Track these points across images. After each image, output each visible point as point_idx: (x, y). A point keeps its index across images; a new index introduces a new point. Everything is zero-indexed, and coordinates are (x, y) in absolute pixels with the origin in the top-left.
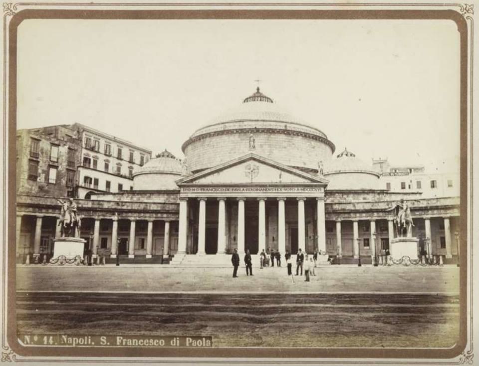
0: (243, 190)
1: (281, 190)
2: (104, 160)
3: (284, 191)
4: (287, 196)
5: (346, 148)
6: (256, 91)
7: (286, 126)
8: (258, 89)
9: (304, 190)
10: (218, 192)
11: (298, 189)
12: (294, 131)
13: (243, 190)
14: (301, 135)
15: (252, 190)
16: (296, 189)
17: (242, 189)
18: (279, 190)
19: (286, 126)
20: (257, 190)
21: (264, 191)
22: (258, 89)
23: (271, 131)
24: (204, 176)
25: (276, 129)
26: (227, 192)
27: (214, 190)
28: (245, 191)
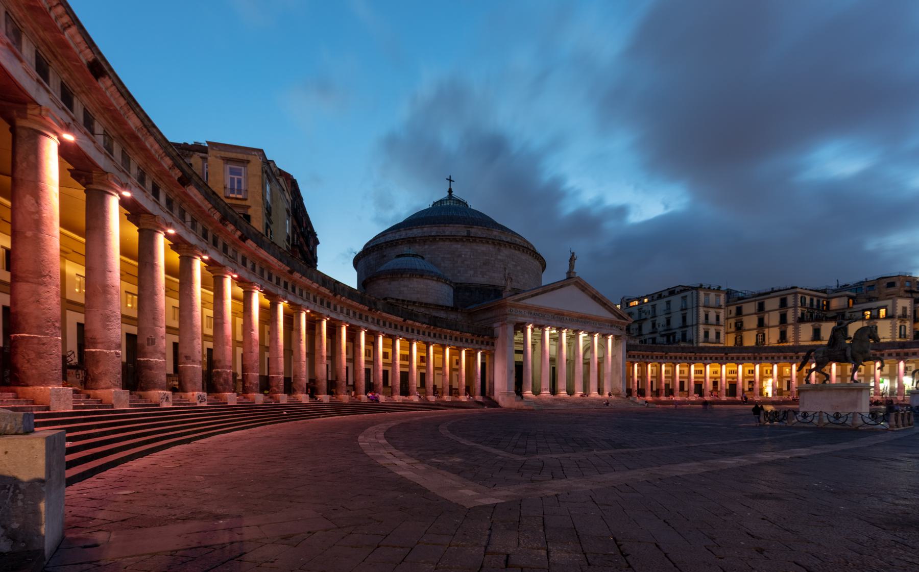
6: (448, 194)
8: (450, 191)
13: (566, 319)
22: (450, 191)
24: (533, 296)
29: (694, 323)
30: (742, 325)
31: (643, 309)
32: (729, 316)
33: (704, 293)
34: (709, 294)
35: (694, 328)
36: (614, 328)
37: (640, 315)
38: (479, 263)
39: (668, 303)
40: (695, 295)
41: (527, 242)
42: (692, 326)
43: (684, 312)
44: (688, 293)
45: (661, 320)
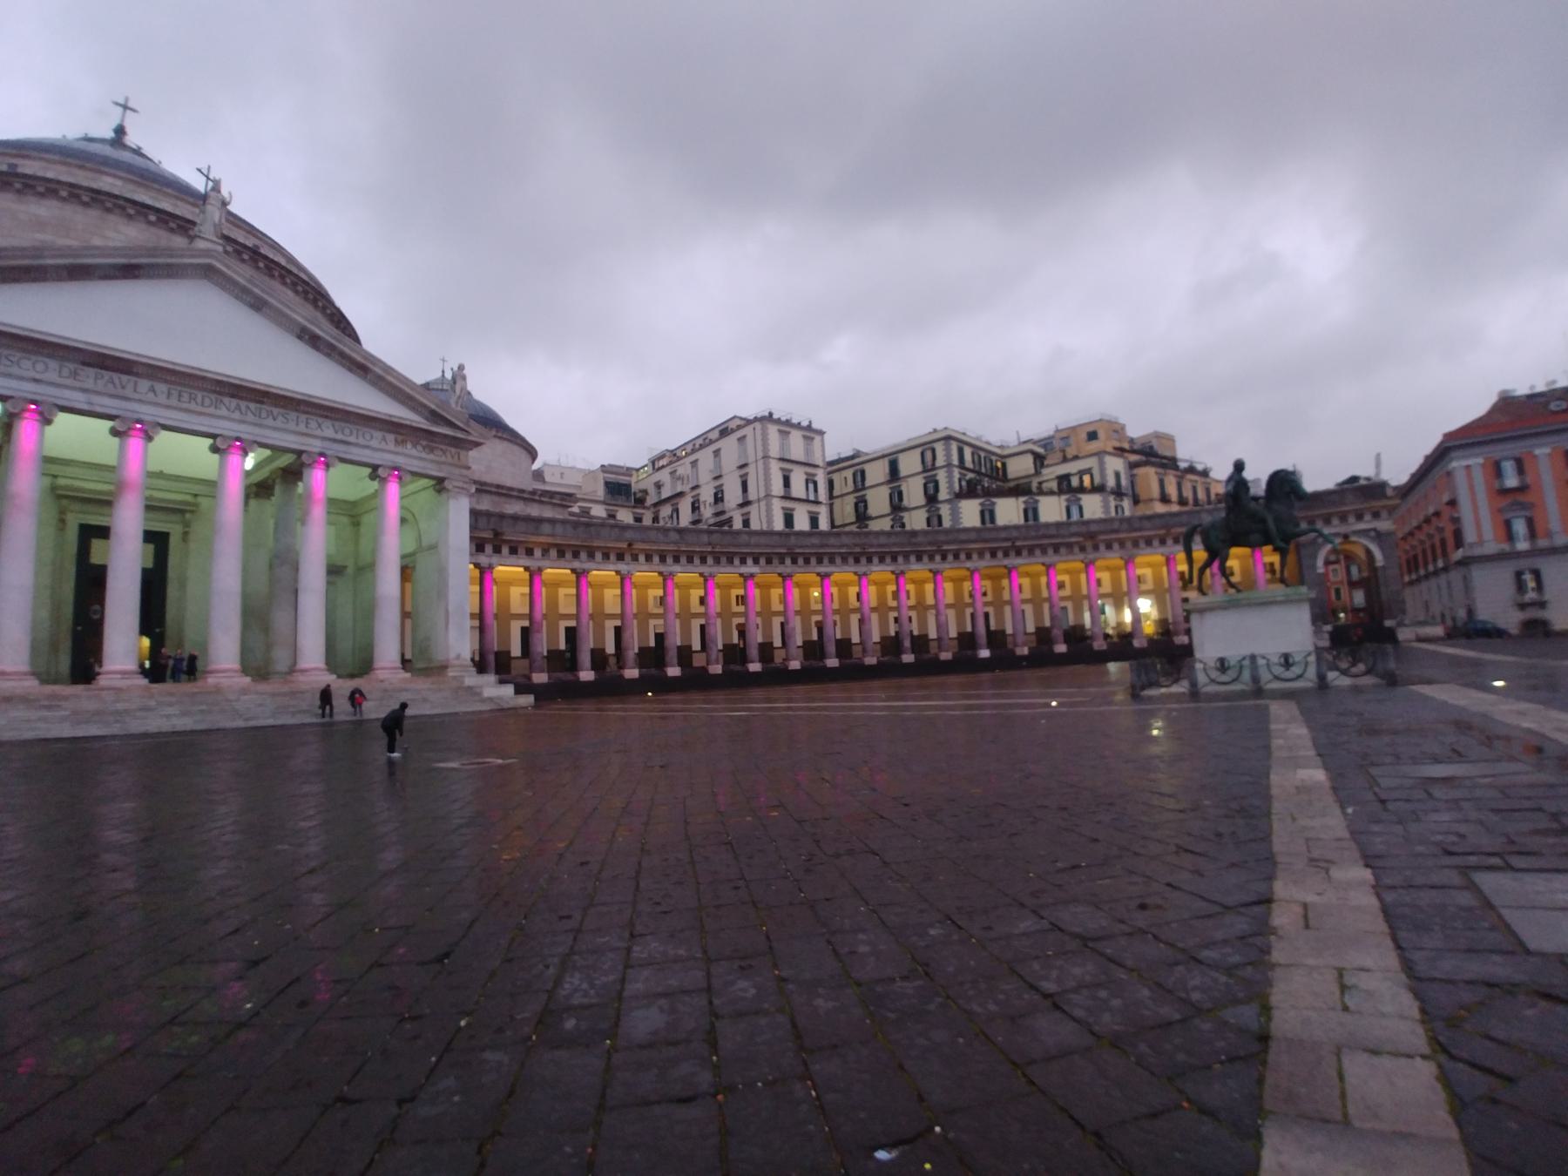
1: (320, 426)
5: (443, 372)
16: (378, 434)
17: (144, 385)
26: (69, 382)
29: (762, 494)
30: (866, 507)
31: (678, 473)
32: (845, 491)
33: (780, 431)
34: (789, 433)
35: (763, 503)
36: (414, 452)
37: (674, 486)
39: (717, 453)
40: (759, 432)
41: (251, 230)
42: (759, 500)
43: (743, 471)
44: (748, 431)
45: (707, 495)
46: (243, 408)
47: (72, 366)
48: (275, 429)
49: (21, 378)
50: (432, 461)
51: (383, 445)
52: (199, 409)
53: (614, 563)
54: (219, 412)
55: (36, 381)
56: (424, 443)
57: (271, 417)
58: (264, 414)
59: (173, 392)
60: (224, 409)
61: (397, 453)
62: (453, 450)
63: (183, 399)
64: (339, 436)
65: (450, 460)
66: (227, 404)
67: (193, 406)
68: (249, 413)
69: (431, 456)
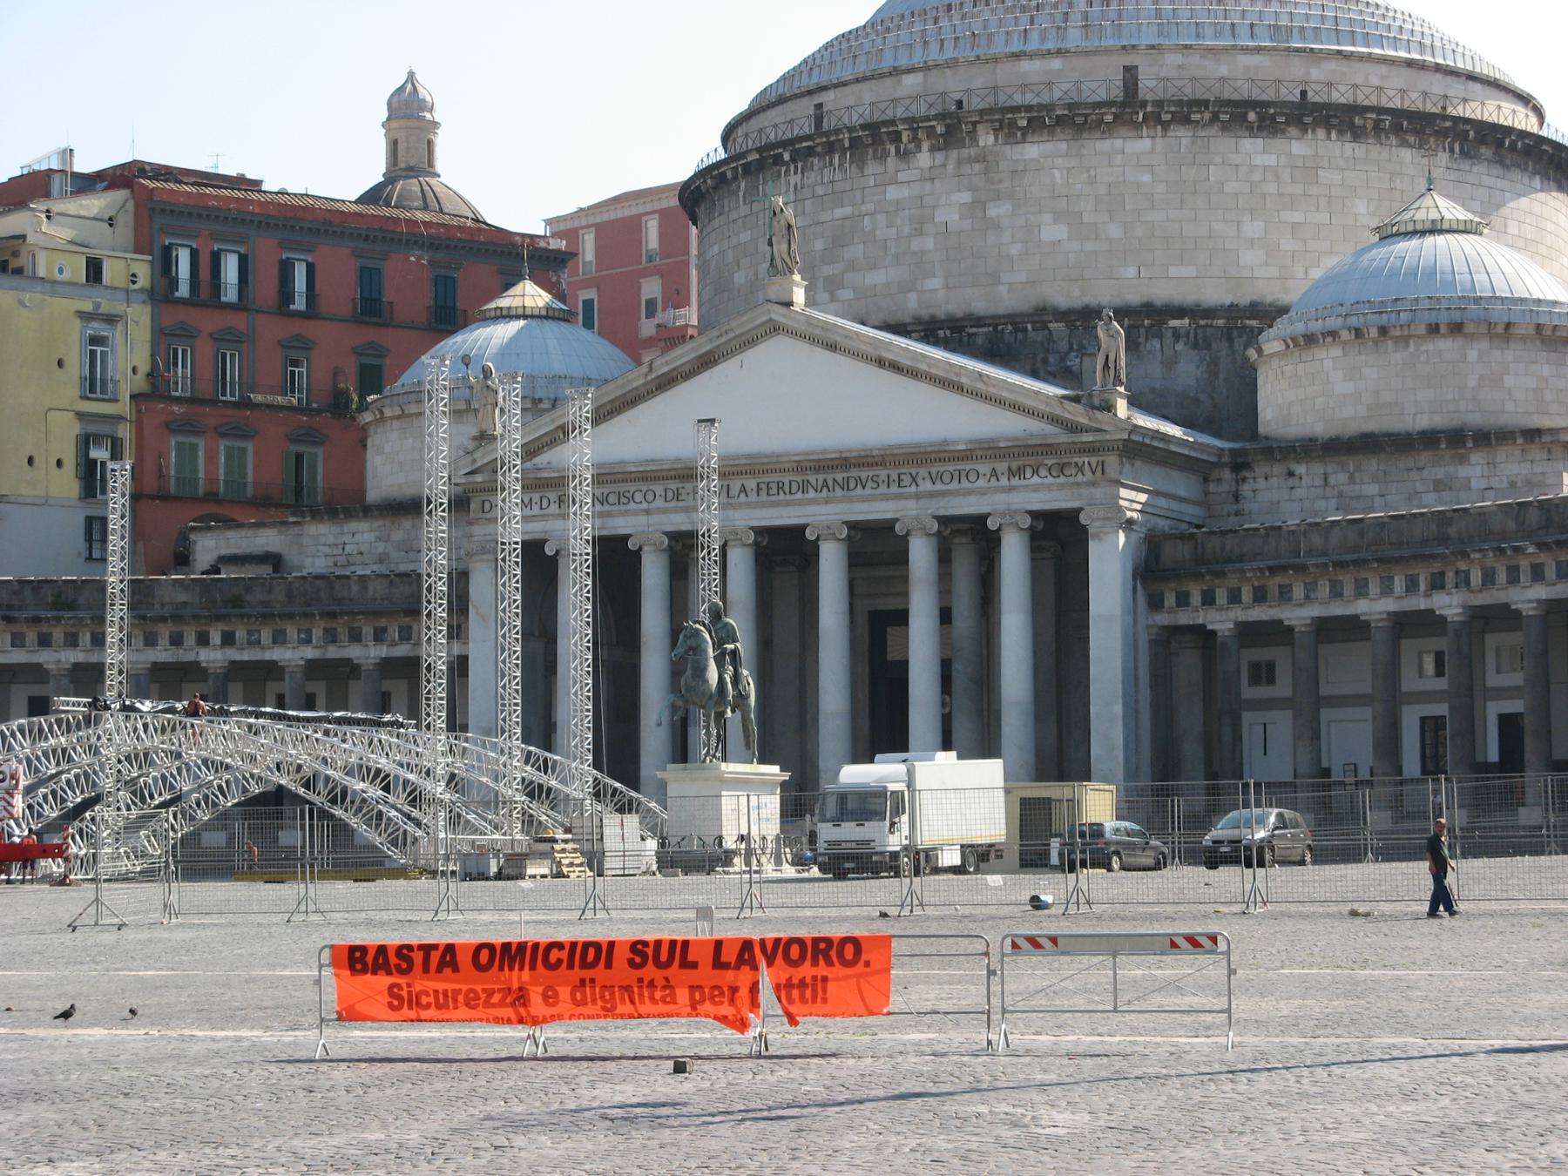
0: (743, 489)
2: (281, 344)
3: (927, 486)
4: (942, 512)
7: (1131, 71)
9: (1019, 472)
10: (632, 506)
11: (994, 473)
12: (1159, 104)
13: (743, 489)
14: (1215, 118)
15: (780, 487)
16: (985, 468)
18: (907, 480)
19: (1131, 71)
20: (804, 487)
21: (839, 492)
23: (1025, 123)
25: (1049, 108)
26: (673, 504)
27: (612, 499)
28: (753, 497)
36: (1036, 479)
38: (819, 245)
46: (830, 483)
47: (674, 485)
48: (866, 499)
49: (635, 513)
50: (1061, 486)
51: (993, 482)
52: (789, 497)
53: (1427, 595)
54: (806, 496)
55: (647, 512)
56: (1050, 462)
57: (859, 486)
58: (852, 485)
59: (762, 486)
60: (811, 490)
61: (1011, 489)
62: (1094, 460)
63: (771, 492)
64: (939, 487)
65: (1089, 476)
66: (814, 484)
67: (782, 496)
68: (837, 487)
69: (1062, 479)
